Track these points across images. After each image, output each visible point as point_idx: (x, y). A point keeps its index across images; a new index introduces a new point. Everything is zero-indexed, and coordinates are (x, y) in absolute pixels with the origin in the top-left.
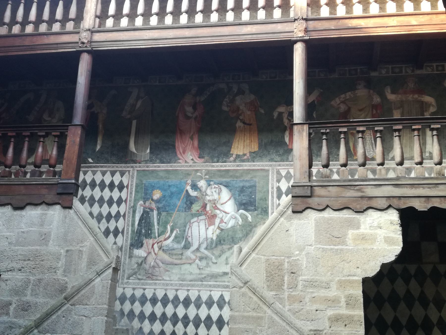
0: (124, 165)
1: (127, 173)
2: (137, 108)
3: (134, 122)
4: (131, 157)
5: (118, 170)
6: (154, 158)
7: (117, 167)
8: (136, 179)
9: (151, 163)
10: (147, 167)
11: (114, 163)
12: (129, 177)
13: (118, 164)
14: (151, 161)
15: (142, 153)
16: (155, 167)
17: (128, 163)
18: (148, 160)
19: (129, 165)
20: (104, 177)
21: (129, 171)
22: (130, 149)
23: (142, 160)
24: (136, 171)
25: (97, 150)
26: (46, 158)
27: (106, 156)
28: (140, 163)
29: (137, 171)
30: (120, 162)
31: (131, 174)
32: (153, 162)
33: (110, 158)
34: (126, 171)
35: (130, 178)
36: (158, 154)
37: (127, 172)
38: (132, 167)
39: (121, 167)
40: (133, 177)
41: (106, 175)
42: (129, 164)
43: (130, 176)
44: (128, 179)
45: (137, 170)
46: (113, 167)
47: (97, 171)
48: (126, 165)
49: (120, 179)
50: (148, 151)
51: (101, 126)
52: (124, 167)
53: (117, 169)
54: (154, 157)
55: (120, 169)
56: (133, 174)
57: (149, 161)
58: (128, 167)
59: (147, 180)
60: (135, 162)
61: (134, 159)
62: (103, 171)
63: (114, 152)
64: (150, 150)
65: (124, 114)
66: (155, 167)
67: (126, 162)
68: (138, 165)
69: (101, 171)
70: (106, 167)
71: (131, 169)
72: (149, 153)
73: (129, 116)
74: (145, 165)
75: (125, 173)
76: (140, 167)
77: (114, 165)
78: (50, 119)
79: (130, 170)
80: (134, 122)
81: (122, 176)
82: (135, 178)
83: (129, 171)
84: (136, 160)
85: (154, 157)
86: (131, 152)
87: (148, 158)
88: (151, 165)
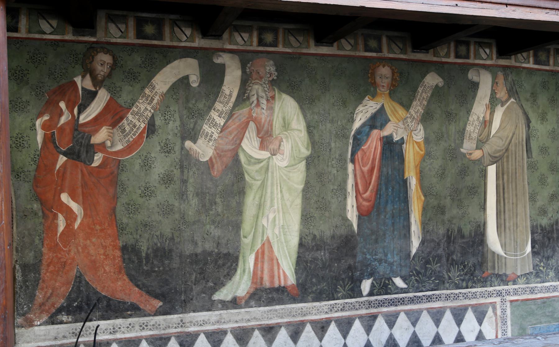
0: (479, 290)
1: (490, 312)
2: (493, 132)
3: (492, 170)
4: (494, 268)
5: (470, 305)
6: (544, 267)
7: (466, 296)
8: (512, 325)
9: (539, 280)
10: (532, 291)
11: (458, 287)
12: (496, 319)
13: (467, 288)
14: (537, 274)
15: (516, 256)
16: (548, 289)
17: (489, 283)
18: (532, 273)
19: (491, 289)
20: (440, 327)
21: (493, 305)
22: (489, 246)
23: (519, 274)
24: (508, 304)
25: (414, 251)
26: (276, 285)
27: (436, 267)
28: (515, 283)
29: (511, 304)
30: (470, 284)
31: (499, 312)
32: (541, 277)
33: (447, 272)
34: (486, 305)
35: (500, 324)
36: (548, 258)
37: (488, 308)
38: (499, 294)
39: (474, 296)
40: (504, 323)
41: (444, 322)
42: (491, 286)
43: (498, 317)
44: (495, 327)
45: (511, 301)
46: (456, 297)
47: (420, 312)
48: (485, 289)
49: (477, 328)
50: (529, 249)
51: (413, 182)
52: (482, 296)
53: (467, 302)
54: (542, 264)
55: (474, 302)
56: (504, 311)
57: (532, 277)
58: (490, 295)
59: (535, 324)
60: (503, 279)
61: (500, 273)
62: (435, 310)
63: (455, 257)
64: (533, 247)
65: (468, 146)
66: (548, 289)
67: (484, 282)
68: (511, 287)
69: (429, 310)
70: (438, 298)
71: (498, 300)
72: (531, 255)
73: (477, 154)
74: (527, 285)
75: (487, 312)
76: (516, 292)
77: (457, 291)
78: (265, 155)
79: (495, 303)
80: (492, 170)
81: (480, 322)
82: (509, 323)
83: (493, 305)
84: (505, 275)
85: (542, 264)
86: (494, 253)
87: (529, 268)
88: (539, 285)
